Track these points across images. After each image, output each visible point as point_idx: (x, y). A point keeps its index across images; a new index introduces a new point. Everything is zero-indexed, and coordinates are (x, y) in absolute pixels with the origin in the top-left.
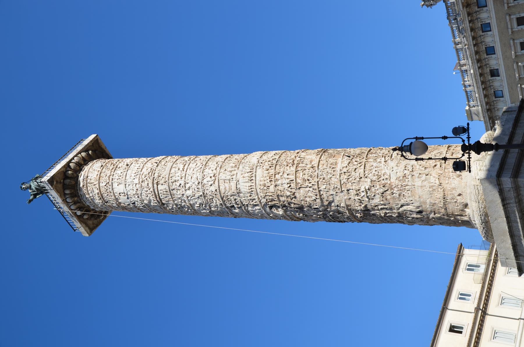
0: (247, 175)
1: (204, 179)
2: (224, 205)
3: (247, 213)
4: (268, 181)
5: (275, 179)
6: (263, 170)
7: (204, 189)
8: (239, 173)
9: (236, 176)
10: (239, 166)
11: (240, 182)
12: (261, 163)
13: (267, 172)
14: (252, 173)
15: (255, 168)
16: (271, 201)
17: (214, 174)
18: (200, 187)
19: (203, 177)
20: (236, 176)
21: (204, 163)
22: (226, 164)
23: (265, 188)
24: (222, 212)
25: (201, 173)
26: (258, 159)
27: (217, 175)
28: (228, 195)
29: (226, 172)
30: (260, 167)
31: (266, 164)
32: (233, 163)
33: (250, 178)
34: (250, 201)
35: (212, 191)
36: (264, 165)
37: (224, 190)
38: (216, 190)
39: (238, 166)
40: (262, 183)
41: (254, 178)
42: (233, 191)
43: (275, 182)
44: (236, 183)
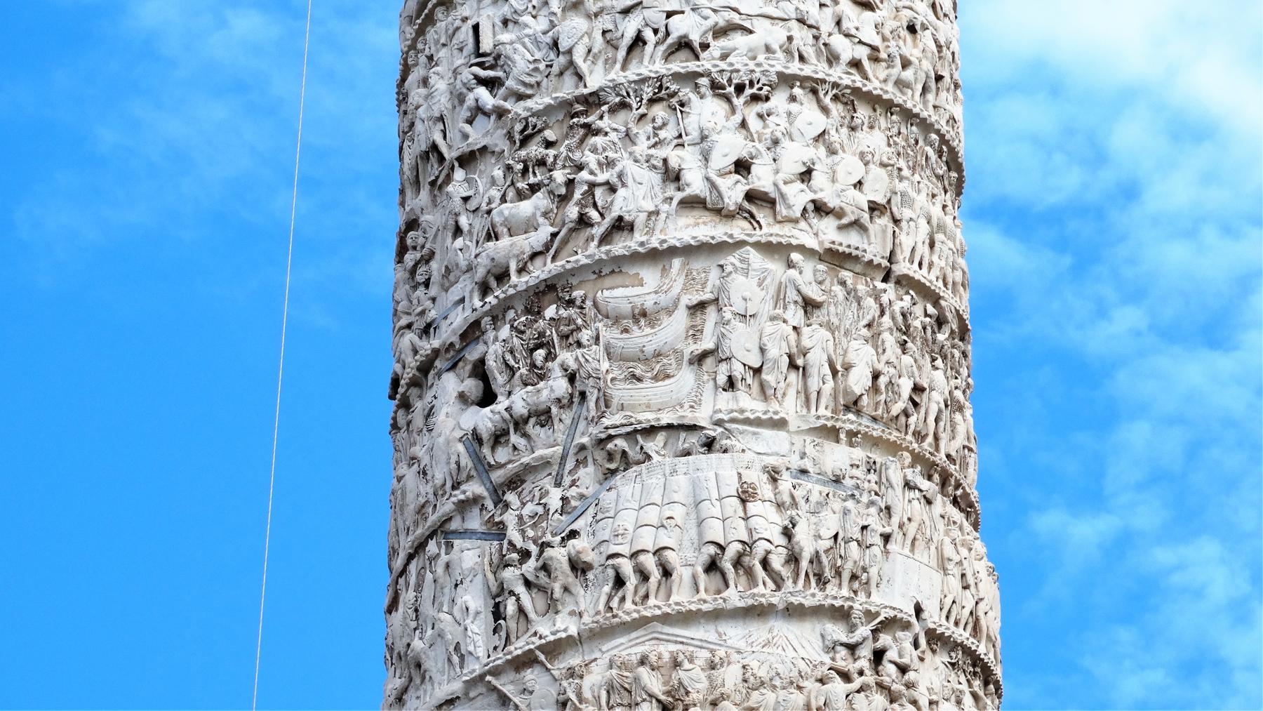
1: (727, 99)
2: (490, 299)
3: (433, 518)
6: (810, 685)
7: (633, 102)
8: (785, 448)
9: (758, 422)
10: (852, 434)
12: (878, 656)
14: (786, 572)
15: (837, 593)
17: (773, 194)
18: (652, 64)
19: (740, 89)
20: (758, 422)
21: (877, 81)
22: (870, 302)
24: (434, 265)
25: (780, 64)
26: (918, 610)
27: (770, 230)
28: (579, 344)
29: (795, 315)
30: (843, 652)
32: (876, 376)
33: (737, 563)
34: (532, 564)
35: (621, 192)
36: (856, 685)
37: (626, 308)
38: (621, 226)
39: (849, 421)
41: (734, 596)
42: (621, 392)
44: (693, 428)
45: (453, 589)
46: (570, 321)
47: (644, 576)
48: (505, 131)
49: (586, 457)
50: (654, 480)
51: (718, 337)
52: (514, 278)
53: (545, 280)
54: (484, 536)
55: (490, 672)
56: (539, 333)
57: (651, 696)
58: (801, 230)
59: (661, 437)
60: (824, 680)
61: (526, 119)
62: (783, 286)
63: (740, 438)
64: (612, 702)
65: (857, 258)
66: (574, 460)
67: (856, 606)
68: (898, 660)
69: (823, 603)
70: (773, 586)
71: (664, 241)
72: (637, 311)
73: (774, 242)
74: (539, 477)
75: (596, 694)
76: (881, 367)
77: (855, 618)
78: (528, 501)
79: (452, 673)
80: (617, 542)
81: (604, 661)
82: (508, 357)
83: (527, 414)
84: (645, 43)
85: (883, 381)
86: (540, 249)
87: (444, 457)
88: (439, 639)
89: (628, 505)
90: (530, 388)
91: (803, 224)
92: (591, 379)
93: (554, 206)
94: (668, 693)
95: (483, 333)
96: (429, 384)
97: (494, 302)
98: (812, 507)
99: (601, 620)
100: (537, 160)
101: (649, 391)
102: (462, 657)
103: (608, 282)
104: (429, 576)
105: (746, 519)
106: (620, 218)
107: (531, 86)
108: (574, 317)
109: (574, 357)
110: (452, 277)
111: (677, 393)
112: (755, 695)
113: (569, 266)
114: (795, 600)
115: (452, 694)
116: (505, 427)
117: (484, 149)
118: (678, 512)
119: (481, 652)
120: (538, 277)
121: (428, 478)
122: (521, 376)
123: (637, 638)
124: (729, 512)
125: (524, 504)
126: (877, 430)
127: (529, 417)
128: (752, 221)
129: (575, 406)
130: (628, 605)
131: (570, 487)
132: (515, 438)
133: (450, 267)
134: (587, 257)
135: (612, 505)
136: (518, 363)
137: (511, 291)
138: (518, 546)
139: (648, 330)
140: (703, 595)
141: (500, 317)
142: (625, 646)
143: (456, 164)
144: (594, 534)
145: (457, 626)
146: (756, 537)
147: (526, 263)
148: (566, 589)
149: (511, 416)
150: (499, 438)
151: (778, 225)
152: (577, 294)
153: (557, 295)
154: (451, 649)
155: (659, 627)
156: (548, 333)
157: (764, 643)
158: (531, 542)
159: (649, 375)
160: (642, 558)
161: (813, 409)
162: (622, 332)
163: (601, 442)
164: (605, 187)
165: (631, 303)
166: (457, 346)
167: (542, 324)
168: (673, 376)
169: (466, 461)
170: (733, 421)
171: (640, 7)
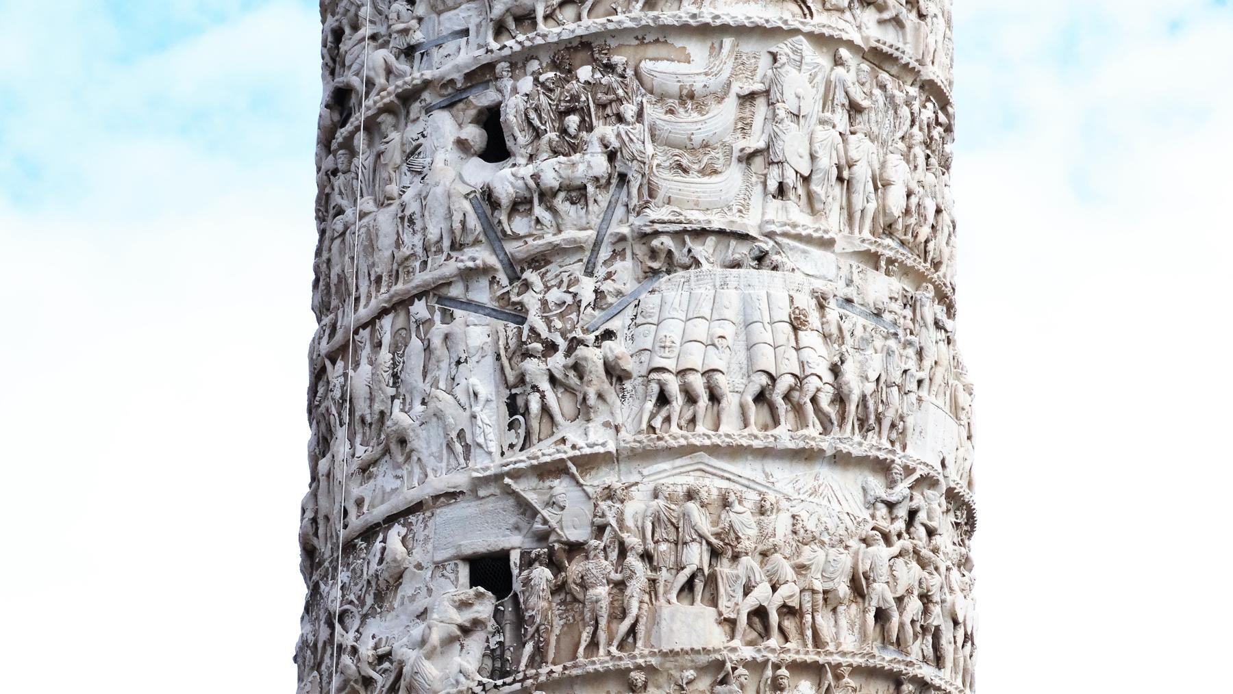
0: (818, 357)
3: (421, 278)
4: (761, 594)
5: (777, 667)
6: (854, 543)
8: (832, 273)
9: (808, 240)
10: (890, 261)
11: (748, 274)
12: (912, 514)
13: (843, 589)
14: (832, 411)
16: (559, 589)
20: (808, 240)
23: (696, 556)
26: (943, 464)
28: (620, 118)
30: (882, 510)
31: (909, 573)
32: (909, 195)
33: (787, 397)
34: (558, 361)
36: (898, 545)
37: (674, 87)
39: (889, 247)
40: (744, 520)
41: (784, 435)
42: (667, 182)
43: (748, 664)
44: (744, 237)
45: (453, 366)
46: (609, 89)
47: (691, 399)
49: (624, 249)
50: (703, 290)
51: (770, 135)
52: (542, 27)
53: (581, 37)
54: (494, 313)
55: (509, 474)
56: (572, 96)
57: (700, 536)
58: (846, 21)
59: (711, 241)
60: (869, 541)
62: (833, 86)
63: (789, 255)
64: (657, 537)
65: (897, 59)
66: (610, 249)
67: (898, 461)
68: (929, 523)
69: (869, 454)
70: (821, 429)
71: (717, 17)
72: (685, 92)
73: (827, 35)
74: (568, 261)
75: (639, 524)
76: (914, 186)
77: (896, 473)
78: (553, 286)
79: (453, 463)
80: (664, 355)
81: (646, 487)
82: (533, 115)
83: (557, 188)
85: (914, 200)
87: (442, 211)
88: (434, 419)
89: (674, 314)
90: (562, 158)
91: (848, 15)
92: (635, 162)
94: (717, 535)
95: (497, 79)
96: (412, 116)
97: (517, 48)
98: (856, 342)
99: (645, 440)
101: (695, 186)
102: (467, 448)
103: (652, 51)
104: (416, 344)
105: (798, 349)
108: (615, 85)
109: (616, 132)
111: (727, 193)
112: (806, 550)
113: (610, 26)
114: (845, 448)
115: (454, 488)
116: (527, 195)
118: (728, 330)
119: (494, 447)
120: (573, 31)
121: (416, 228)
122: (550, 141)
123: (682, 466)
124: (781, 339)
125: (548, 288)
126: (911, 260)
127: (559, 190)
128: (802, 5)
129: (613, 187)
130: (674, 428)
131: (605, 279)
132: (539, 211)
134: (632, 19)
135: (656, 310)
136: (544, 124)
137: (539, 41)
138: (543, 336)
139: (695, 116)
140: (753, 429)
141: (520, 65)
142: (668, 474)
144: (632, 338)
145: (461, 410)
146: (808, 372)
147: (555, 10)
148: (600, 396)
149: (538, 185)
150: (520, 205)
151: (826, 13)
152: (617, 59)
153: (592, 55)
154: (454, 435)
155: (706, 458)
156: (583, 98)
157: (810, 491)
158: (559, 334)
159: (696, 167)
161: (856, 230)
162: (666, 113)
163: (644, 237)
165: (679, 81)
166: (459, 85)
167: (576, 86)
168: (720, 172)
169: (473, 222)
170: (785, 235)
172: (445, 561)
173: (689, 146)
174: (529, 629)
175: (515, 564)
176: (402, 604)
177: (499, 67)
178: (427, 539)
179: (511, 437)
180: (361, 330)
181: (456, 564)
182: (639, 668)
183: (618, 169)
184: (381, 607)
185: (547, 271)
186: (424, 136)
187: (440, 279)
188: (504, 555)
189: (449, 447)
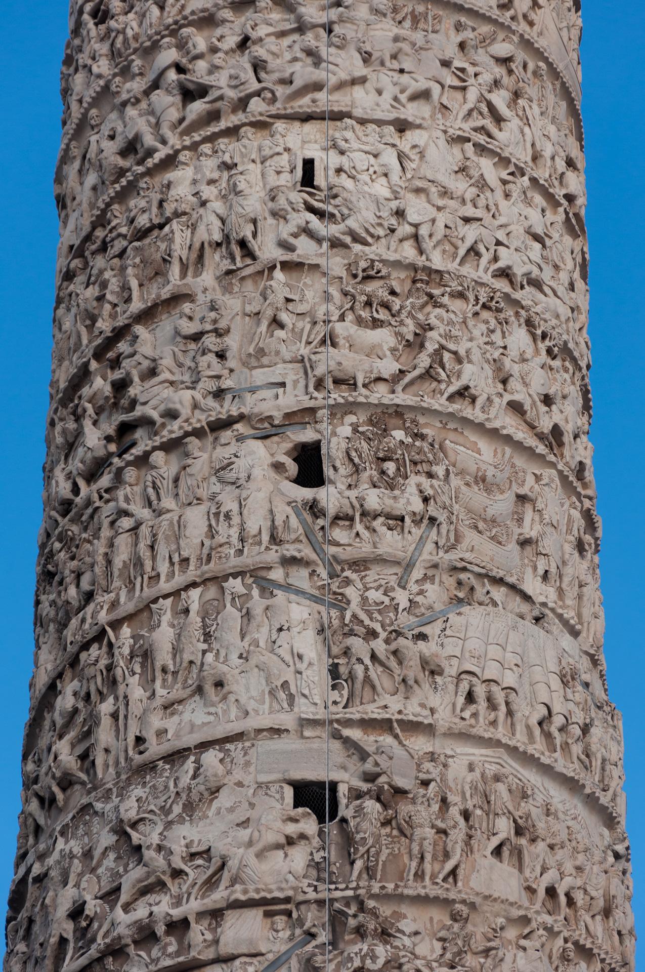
11: (528, 625)
19: (544, 336)
23: (504, 828)
34: (379, 645)
45: (274, 632)
47: (492, 705)
48: (346, 262)
49: (434, 576)
53: (398, 406)
61: (373, 261)
66: (423, 572)
72: (480, 474)
74: (385, 572)
78: (371, 588)
84: (478, 254)
86: (386, 376)
88: (256, 670)
93: (401, 347)
95: (316, 422)
100: (382, 301)
102: (291, 698)
106: (467, 388)
107: (372, 236)
110: (265, 360)
116: (350, 512)
117: (316, 267)
121: (232, 523)
122: (371, 477)
123: (487, 756)
132: (359, 527)
133: (266, 351)
141: (339, 416)
143: (278, 266)
145: (285, 666)
149: (362, 506)
160: (495, 688)
164: (452, 356)
171: (479, 223)
172: (269, 782)
173: (483, 516)
174: (361, 848)
175: (344, 795)
176: (218, 813)
177: (320, 413)
178: (248, 764)
179: (335, 696)
180: (161, 600)
181: (282, 787)
182: (463, 902)
183: (429, 513)
184: (191, 816)
185: (366, 576)
186: (237, 457)
187: (260, 563)
188: (334, 786)
189: (272, 693)
